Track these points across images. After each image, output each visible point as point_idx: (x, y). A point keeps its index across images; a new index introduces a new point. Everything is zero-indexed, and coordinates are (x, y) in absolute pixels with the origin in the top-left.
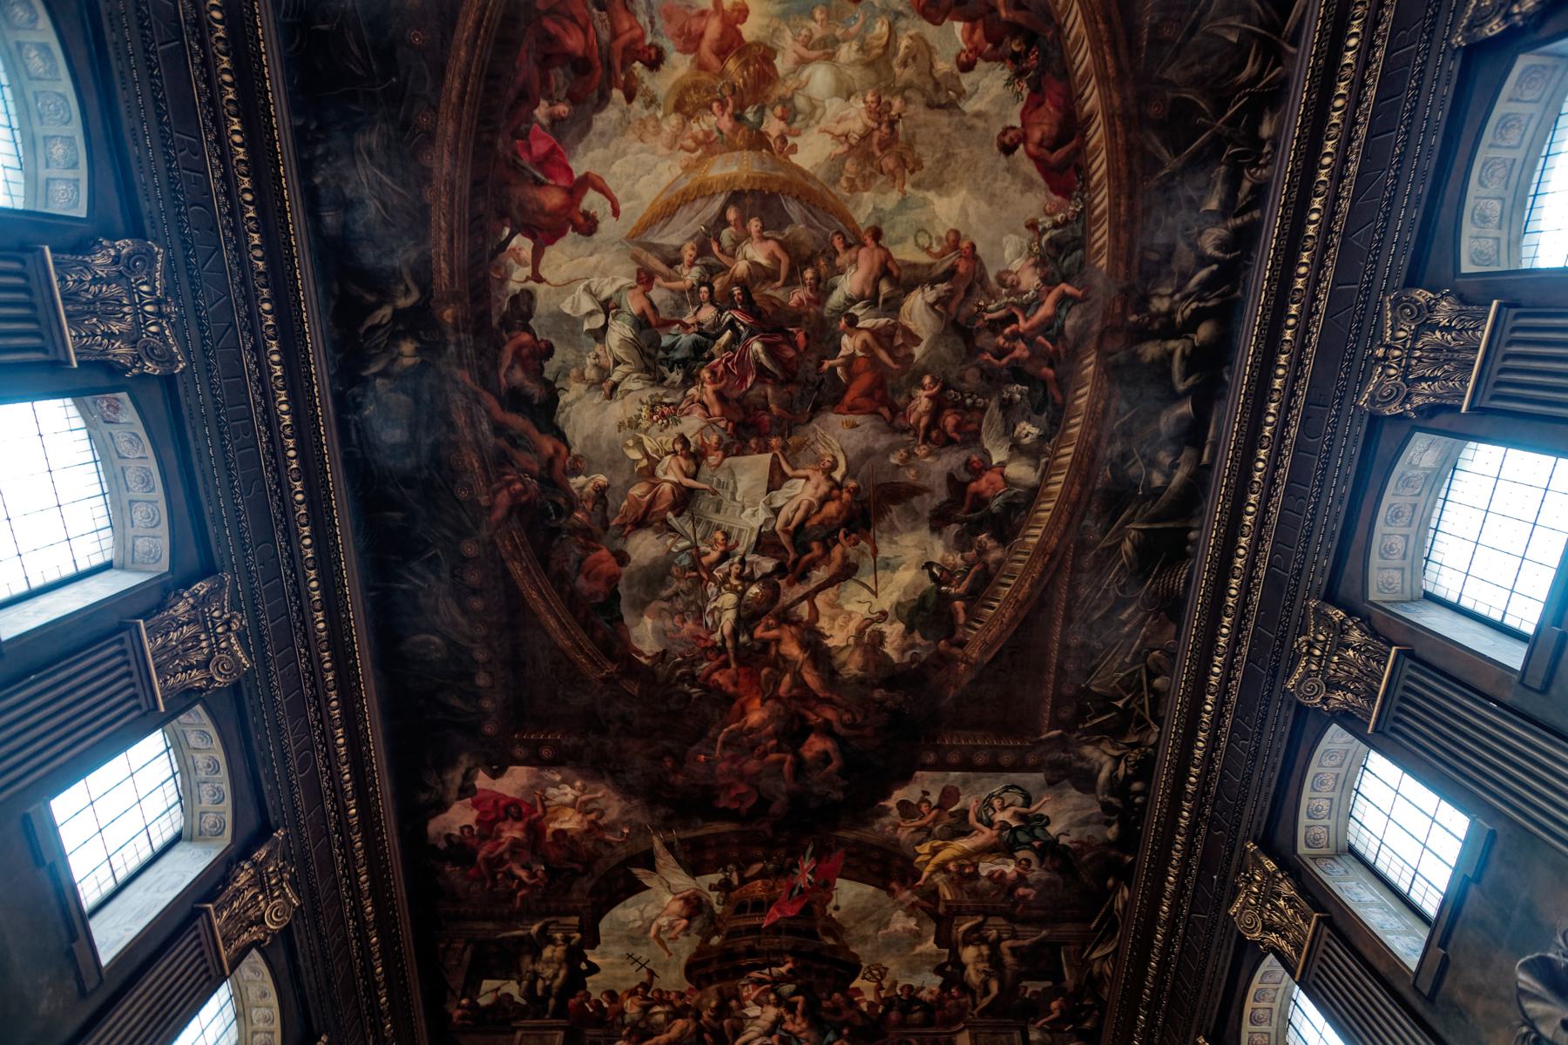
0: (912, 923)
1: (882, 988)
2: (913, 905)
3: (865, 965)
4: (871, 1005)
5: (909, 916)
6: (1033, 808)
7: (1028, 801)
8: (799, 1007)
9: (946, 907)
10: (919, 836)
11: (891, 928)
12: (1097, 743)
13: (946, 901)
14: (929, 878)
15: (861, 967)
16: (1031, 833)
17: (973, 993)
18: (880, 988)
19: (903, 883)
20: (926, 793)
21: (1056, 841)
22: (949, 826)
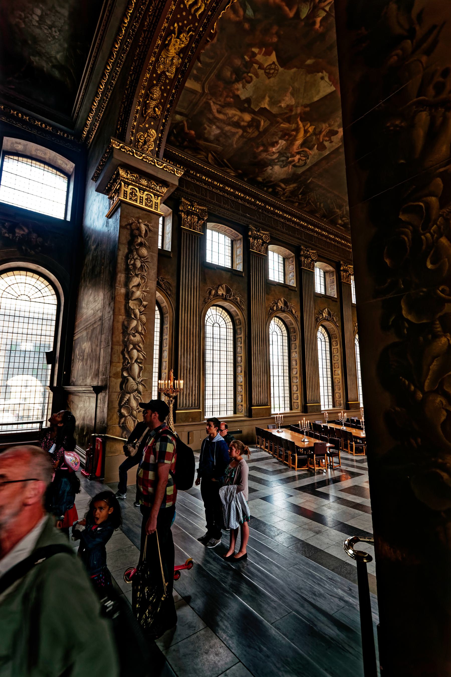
0: (283, 105)
1: (259, 68)
2: (291, 110)
3: (281, 69)
4: (254, 55)
5: (288, 106)
6: (291, 166)
7: (294, 166)
8: (287, 9)
9: (278, 122)
10: (318, 130)
11: (289, 94)
12: (294, 188)
13: (281, 123)
14: (297, 123)
15: (282, 67)
16: (283, 161)
17: (223, 106)
18: (261, 67)
19: (305, 113)
20: (331, 142)
21: (271, 166)
22: (312, 141)
